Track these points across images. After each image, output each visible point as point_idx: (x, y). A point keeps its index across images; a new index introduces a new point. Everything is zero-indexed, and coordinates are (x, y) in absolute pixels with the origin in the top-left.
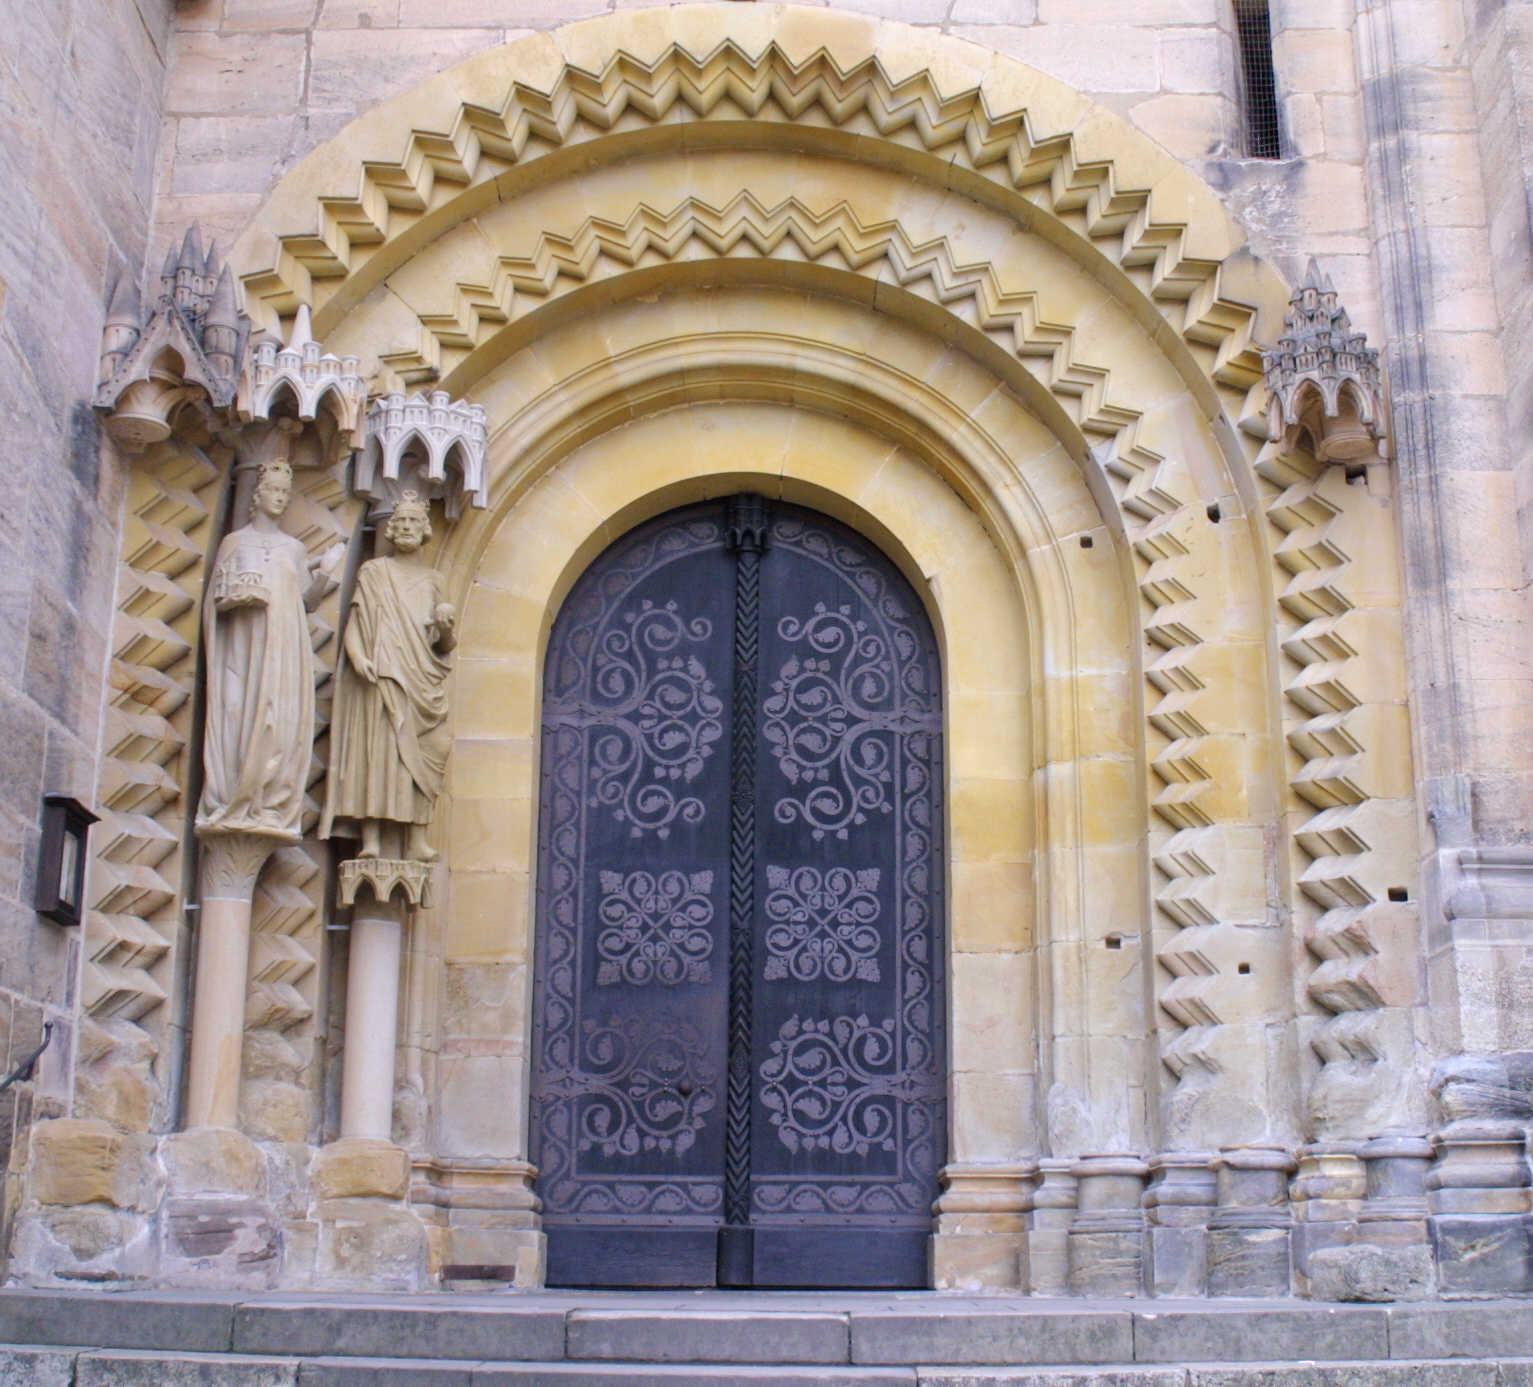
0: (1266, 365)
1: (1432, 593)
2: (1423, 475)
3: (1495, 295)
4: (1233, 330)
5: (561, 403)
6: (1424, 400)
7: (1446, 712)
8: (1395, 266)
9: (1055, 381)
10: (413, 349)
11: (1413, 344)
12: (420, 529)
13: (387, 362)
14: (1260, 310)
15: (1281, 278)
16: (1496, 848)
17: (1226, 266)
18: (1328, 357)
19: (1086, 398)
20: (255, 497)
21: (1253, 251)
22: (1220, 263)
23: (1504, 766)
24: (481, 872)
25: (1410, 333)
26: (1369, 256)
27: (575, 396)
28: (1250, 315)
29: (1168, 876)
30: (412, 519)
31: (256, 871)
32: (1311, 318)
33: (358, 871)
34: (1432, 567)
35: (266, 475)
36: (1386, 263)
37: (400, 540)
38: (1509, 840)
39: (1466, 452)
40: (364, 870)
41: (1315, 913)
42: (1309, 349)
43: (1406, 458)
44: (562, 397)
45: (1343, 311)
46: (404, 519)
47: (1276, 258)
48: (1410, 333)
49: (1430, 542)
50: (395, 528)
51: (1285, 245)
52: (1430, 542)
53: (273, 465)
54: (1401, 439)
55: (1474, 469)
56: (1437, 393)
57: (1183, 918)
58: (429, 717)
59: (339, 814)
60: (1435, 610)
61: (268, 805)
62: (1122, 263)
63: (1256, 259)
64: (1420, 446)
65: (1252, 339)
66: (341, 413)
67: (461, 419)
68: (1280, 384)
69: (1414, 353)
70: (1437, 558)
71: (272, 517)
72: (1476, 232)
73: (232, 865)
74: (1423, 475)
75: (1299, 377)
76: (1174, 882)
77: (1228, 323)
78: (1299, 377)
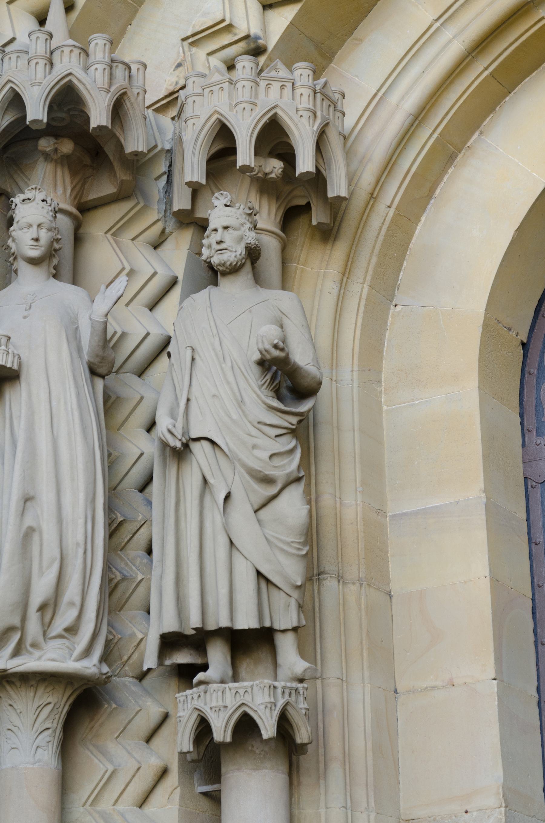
5: (450, 41)
10: (220, 18)
12: (241, 239)
13: (192, 44)
20: (10, 242)
24: (434, 688)
27: (464, 29)
30: (226, 228)
31: (57, 724)
33: (190, 706)
35: (17, 211)
37: (215, 260)
40: (200, 704)
44: (448, 34)
46: (216, 230)
50: (210, 247)
53: (22, 197)
58: (268, 480)
59: (161, 633)
61: (53, 634)
66: (90, 111)
67: (276, 86)
71: (34, 262)
73: (17, 722)
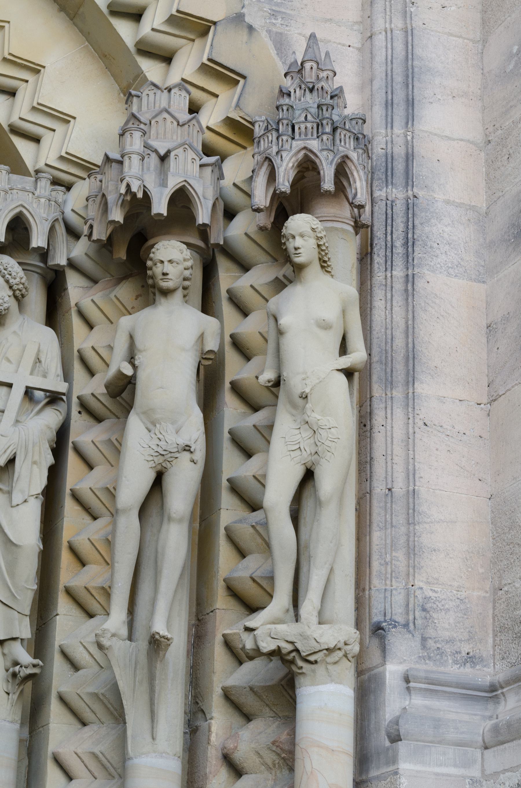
0: (258, 131)
1: (398, 393)
2: (399, 272)
3: (484, 108)
4: (217, 96)
6: (407, 199)
7: (400, 519)
8: (390, 61)
9: (15, 119)
11: (400, 141)
14: (248, 79)
15: (273, 52)
16: (442, 669)
17: (219, 27)
18: (328, 129)
19: (45, 142)
21: (248, 19)
22: (215, 23)
23: (456, 584)
25: (398, 130)
26: (359, 49)
28: (238, 82)
29: (75, 667)
32: (311, 90)
34: (399, 367)
36: (380, 57)
38: (455, 662)
39: (444, 256)
41: (237, 720)
42: (309, 117)
43: (382, 253)
45: (341, 89)
47: (269, 32)
48: (398, 130)
49: (399, 342)
51: (279, 21)
52: (399, 342)
54: (379, 233)
55: (449, 275)
56: (421, 193)
57: (88, 715)
60: (399, 413)
62: (109, 6)
63: (250, 28)
64: (398, 243)
65: (237, 105)
68: (275, 149)
69: (399, 151)
70: (407, 359)
72: (471, 44)
74: (399, 272)
75: (297, 144)
76: (81, 672)
77: (212, 86)
78: (297, 144)
